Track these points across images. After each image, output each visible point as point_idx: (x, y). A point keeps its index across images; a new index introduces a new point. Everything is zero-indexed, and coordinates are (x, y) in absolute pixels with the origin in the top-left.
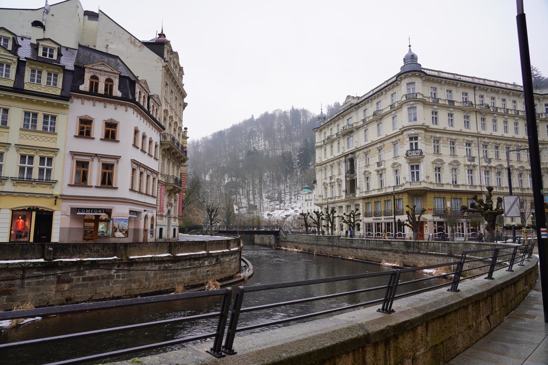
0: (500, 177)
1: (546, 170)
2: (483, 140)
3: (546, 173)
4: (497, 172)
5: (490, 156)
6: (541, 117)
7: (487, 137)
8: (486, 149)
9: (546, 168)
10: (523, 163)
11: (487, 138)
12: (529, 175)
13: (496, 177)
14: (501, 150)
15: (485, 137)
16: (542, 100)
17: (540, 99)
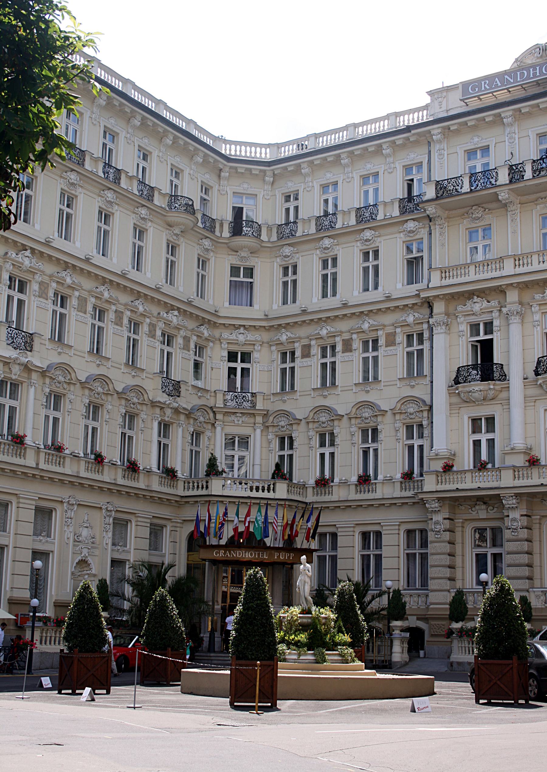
0: (57, 414)
1: (211, 415)
2: (12, 254)
3: (210, 426)
4: (48, 390)
5: (29, 326)
6: (218, 233)
7: (33, 250)
8: (22, 296)
9: (211, 408)
10: (144, 375)
11: (28, 253)
12: (156, 425)
13: (43, 412)
14: (74, 313)
15: (24, 248)
16: (228, 179)
17: (223, 174)
